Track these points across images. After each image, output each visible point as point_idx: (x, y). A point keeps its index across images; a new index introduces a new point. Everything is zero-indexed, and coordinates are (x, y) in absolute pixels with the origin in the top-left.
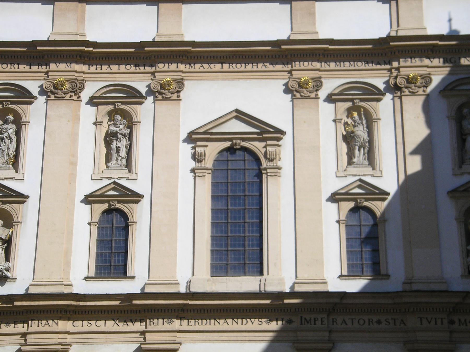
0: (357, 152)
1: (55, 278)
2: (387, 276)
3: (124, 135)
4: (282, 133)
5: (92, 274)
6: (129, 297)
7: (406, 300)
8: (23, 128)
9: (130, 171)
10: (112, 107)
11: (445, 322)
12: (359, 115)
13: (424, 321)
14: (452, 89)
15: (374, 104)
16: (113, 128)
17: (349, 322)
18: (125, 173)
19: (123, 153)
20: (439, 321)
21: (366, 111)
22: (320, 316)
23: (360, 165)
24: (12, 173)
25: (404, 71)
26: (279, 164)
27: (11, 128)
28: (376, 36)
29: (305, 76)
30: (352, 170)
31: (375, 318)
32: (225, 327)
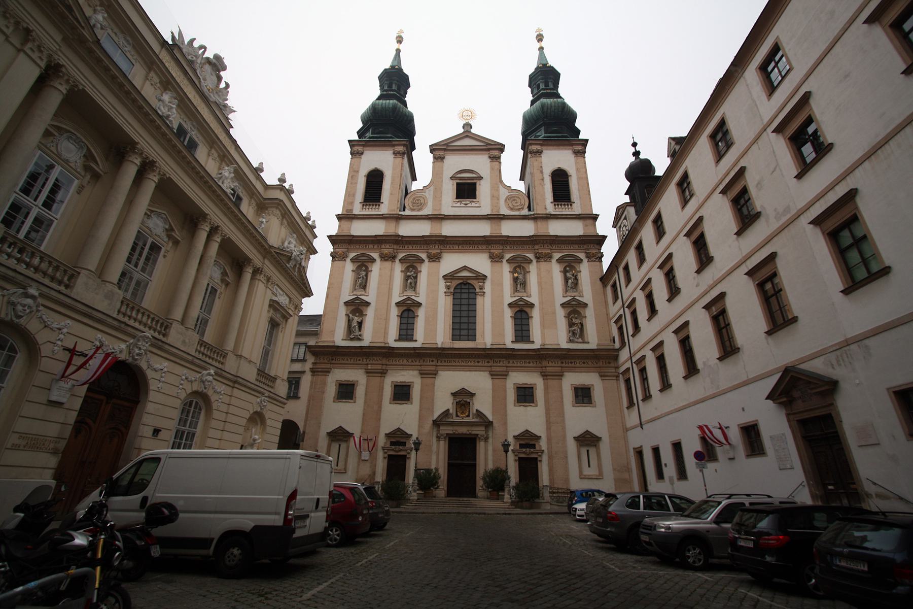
0: (519, 286)
1: (381, 340)
2: (533, 342)
3: (414, 277)
4: (486, 276)
5: (397, 339)
6: (414, 349)
7: (542, 353)
8: (369, 273)
9: (416, 293)
10: (408, 264)
11: (559, 362)
12: (520, 269)
13: (550, 363)
14: (562, 259)
15: (527, 265)
16: (408, 274)
17: (516, 363)
18: (413, 293)
19: (413, 285)
20: (556, 362)
21: (523, 267)
22: (502, 360)
23: (520, 292)
24: (363, 293)
25: (540, 251)
26: (484, 291)
27: (364, 273)
28: (528, 235)
29: (496, 252)
30: (517, 294)
31: (528, 361)
32: (458, 364)
